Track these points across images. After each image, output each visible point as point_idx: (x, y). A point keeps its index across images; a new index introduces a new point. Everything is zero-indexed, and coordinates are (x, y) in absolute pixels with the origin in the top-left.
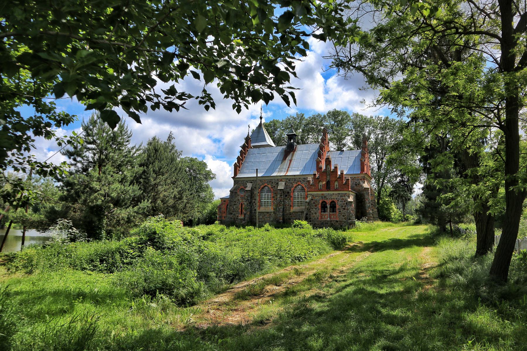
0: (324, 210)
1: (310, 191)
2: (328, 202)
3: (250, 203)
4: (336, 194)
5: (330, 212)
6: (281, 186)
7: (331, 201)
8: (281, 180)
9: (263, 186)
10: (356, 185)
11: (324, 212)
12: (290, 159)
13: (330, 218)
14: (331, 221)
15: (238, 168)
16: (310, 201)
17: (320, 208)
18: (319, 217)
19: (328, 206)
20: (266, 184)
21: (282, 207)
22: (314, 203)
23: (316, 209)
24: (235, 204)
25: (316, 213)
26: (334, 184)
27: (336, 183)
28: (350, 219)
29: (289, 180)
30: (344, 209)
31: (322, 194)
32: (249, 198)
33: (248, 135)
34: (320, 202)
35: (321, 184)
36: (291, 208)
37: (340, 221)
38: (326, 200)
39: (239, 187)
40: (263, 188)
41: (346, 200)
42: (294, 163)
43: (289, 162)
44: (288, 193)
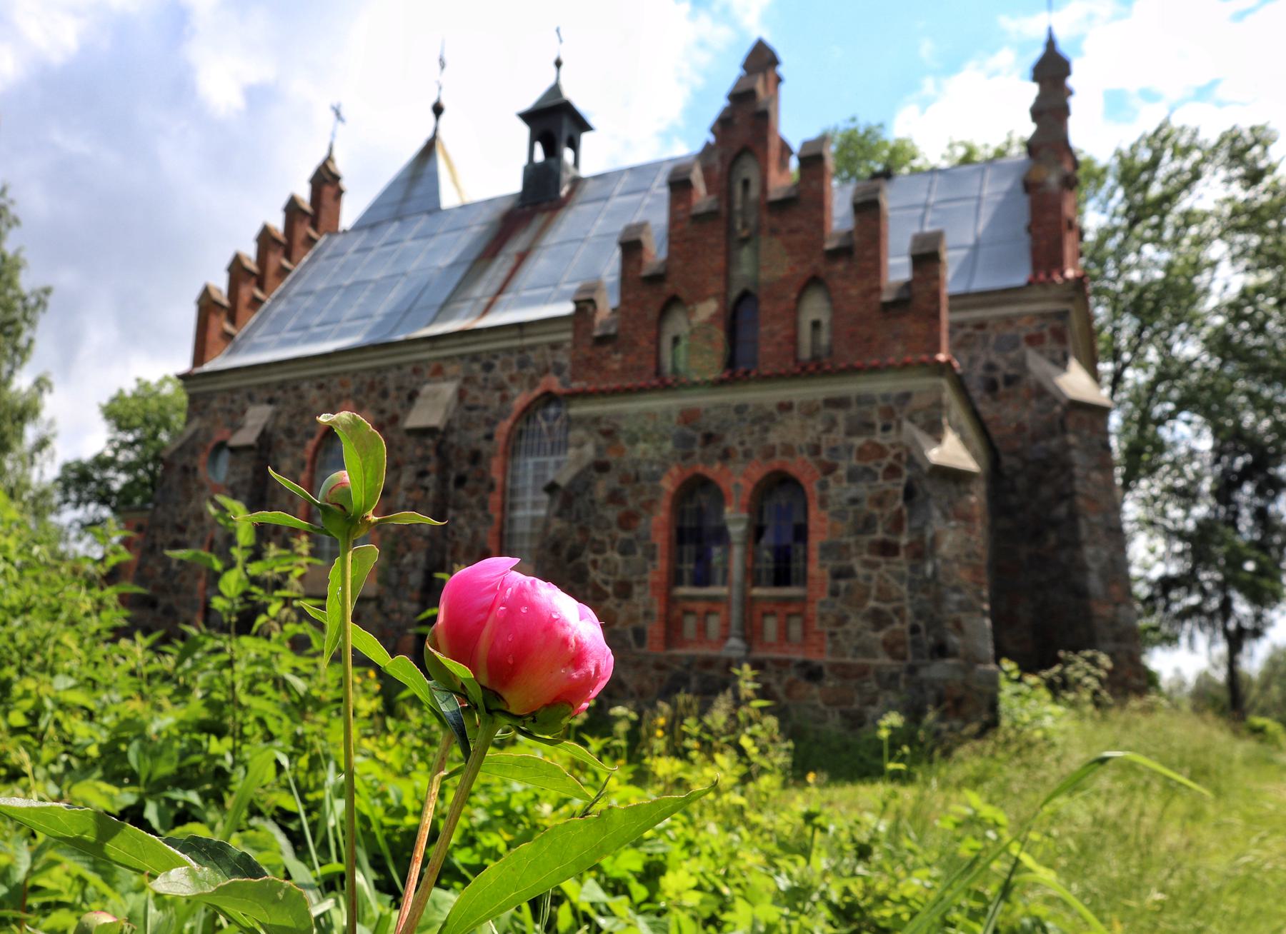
0: (702, 558)
1: (584, 395)
2: (738, 480)
4: (810, 411)
5: (753, 577)
6: (431, 410)
7: (758, 471)
8: (438, 372)
11: (703, 579)
15: (220, 324)
16: (582, 483)
17: (661, 539)
19: (736, 521)
21: (422, 557)
23: (627, 549)
26: (795, 312)
27: (815, 308)
28: (941, 651)
29: (479, 354)
30: (887, 549)
31: (689, 417)
34: (668, 485)
37: (844, 672)
38: (713, 470)
39: (208, 437)
41: (912, 459)
42: (539, 266)
43: (510, 264)
44: (476, 457)
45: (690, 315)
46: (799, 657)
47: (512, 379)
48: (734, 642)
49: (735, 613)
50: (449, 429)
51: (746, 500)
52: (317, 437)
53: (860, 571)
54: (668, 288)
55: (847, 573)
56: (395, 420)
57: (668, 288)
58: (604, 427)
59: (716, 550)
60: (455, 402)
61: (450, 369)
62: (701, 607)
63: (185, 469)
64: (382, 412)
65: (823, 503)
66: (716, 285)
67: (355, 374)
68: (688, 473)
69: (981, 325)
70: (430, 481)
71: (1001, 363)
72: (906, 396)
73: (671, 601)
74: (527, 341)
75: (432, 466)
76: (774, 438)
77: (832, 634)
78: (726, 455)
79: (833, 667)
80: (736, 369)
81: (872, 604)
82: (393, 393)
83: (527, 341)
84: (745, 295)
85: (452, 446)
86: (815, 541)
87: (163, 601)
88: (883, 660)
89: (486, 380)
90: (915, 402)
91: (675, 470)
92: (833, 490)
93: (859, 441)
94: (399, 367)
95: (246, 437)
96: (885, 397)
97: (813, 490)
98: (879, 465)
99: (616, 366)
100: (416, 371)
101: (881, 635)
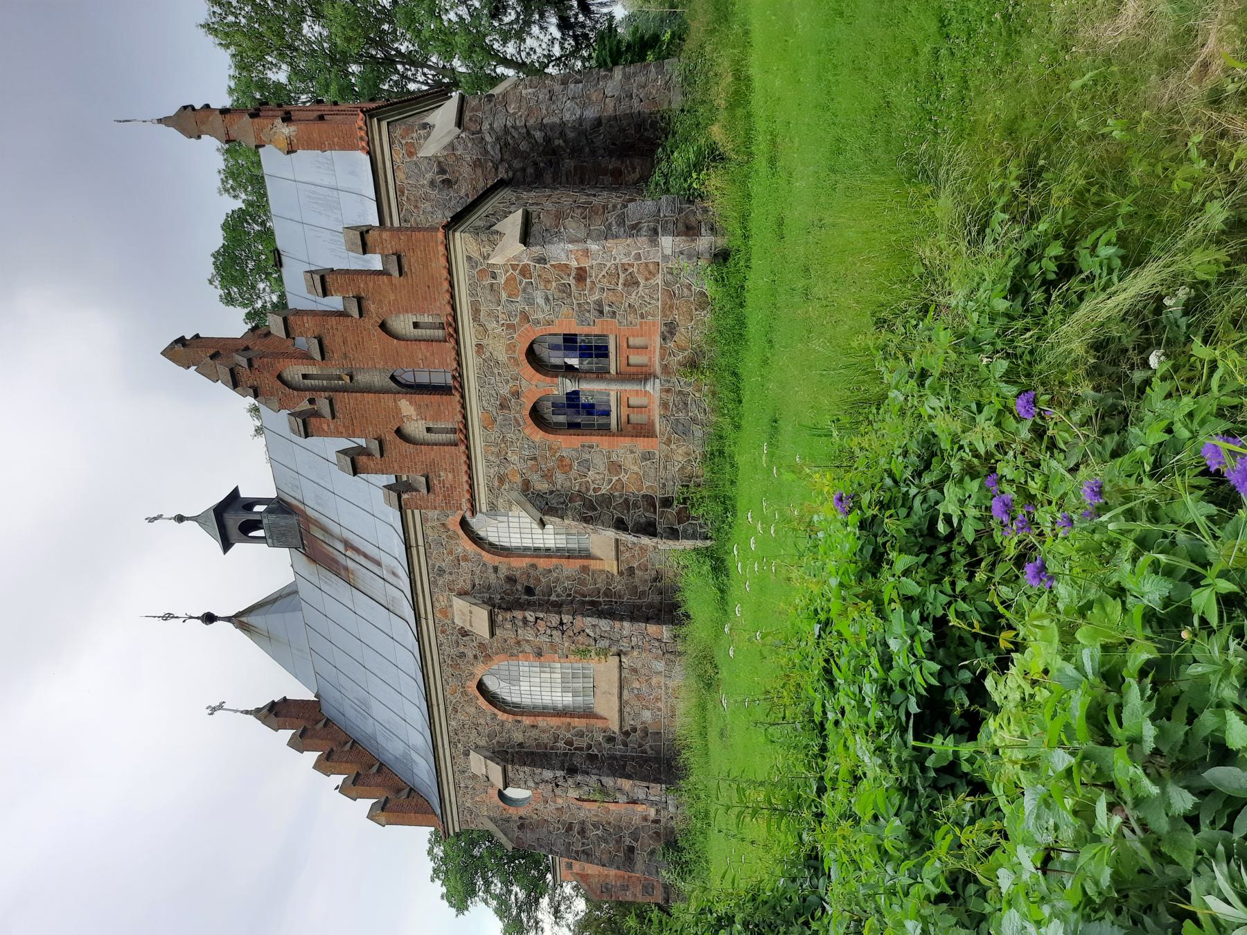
3: (572, 771)
7: (528, 370)
9: (482, 702)
10: (448, 183)
12: (341, 547)
13: (643, 376)
14: (665, 368)
18: (642, 444)
20: (474, 684)
21: (590, 621)
22: (547, 476)
24: (582, 832)
25: (615, 467)
30: (581, 275)
32: (548, 774)
33: (257, 713)
34: (539, 436)
35: (416, 428)
36: (594, 565)
40: (492, 699)
45: (409, 418)
46: (658, 340)
47: (451, 553)
48: (649, 387)
49: (628, 387)
50: (490, 603)
51: (548, 379)
52: (496, 711)
53: (596, 297)
54: (390, 437)
55: (599, 304)
56: (482, 646)
57: (390, 437)
58: (496, 484)
59: (583, 400)
60: (468, 598)
61: (442, 601)
62: (625, 411)
63: (521, 827)
64: (475, 657)
65: (550, 323)
66: (387, 399)
67: (445, 682)
68: (530, 421)
69: (400, 191)
70: (531, 616)
71: (429, 176)
72: (469, 258)
73: (621, 432)
74: (421, 542)
75: (518, 614)
76: (502, 357)
77: (642, 317)
78: (517, 394)
79: (664, 315)
80: (453, 388)
81: (620, 287)
82: (462, 649)
83: (421, 542)
84: (393, 378)
85: (502, 598)
86: (575, 328)
87: (628, 841)
88: (659, 280)
89: (451, 573)
90: (475, 255)
91: (527, 431)
92: (540, 316)
93: (504, 295)
94: (439, 646)
95: (496, 772)
96: (471, 277)
97: (538, 331)
98: (521, 283)
99: (450, 476)
100: (443, 632)
101: (642, 281)
